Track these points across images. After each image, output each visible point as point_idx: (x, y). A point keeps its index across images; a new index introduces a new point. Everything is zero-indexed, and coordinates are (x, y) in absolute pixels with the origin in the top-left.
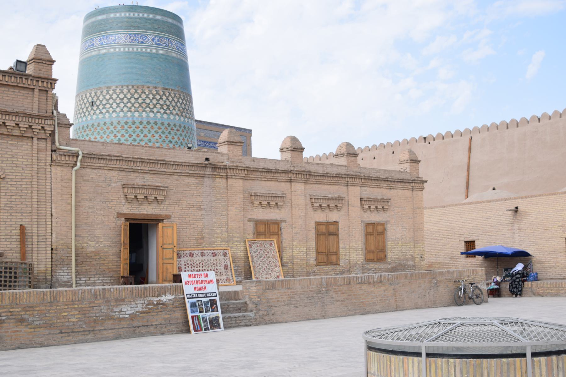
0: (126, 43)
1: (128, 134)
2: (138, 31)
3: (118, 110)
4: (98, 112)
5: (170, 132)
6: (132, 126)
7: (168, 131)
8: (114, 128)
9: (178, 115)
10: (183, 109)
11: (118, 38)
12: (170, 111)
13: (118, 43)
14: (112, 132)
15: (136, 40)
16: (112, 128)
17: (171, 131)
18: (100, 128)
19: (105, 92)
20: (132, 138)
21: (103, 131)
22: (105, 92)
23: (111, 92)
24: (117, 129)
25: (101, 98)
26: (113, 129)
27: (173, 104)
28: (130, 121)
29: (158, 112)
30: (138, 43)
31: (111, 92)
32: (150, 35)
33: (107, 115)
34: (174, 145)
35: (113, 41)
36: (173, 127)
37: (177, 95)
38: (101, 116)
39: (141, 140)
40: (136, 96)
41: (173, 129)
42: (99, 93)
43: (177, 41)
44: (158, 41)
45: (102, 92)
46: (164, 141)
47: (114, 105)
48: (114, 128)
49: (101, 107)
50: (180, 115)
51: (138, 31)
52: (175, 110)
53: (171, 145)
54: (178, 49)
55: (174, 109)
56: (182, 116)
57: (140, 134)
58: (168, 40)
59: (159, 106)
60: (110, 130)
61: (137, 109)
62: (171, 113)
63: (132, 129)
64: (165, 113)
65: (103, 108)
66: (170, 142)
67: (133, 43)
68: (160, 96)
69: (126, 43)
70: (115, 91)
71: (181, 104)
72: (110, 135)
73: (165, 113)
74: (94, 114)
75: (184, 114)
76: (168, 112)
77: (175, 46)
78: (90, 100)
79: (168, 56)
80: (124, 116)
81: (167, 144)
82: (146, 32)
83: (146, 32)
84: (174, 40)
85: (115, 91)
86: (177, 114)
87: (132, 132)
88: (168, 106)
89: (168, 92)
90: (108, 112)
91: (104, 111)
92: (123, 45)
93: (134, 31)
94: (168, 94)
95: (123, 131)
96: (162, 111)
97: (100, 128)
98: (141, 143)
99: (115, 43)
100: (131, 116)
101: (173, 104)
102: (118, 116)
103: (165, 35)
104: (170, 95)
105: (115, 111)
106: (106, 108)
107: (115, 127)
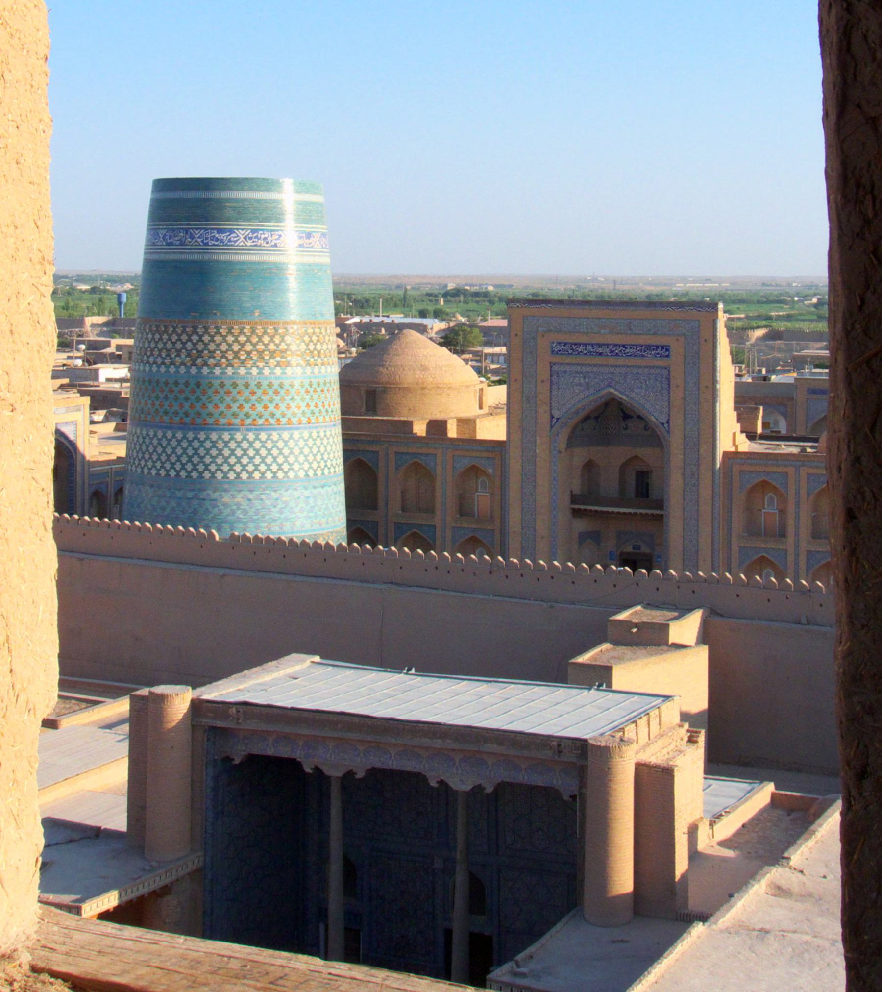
5: (166, 395)
7: (165, 393)
9: (185, 364)
10: (198, 351)
12: (171, 358)
17: (168, 394)
27: (179, 345)
29: (155, 362)
32: (162, 229)
34: (171, 418)
36: (173, 386)
37: (187, 330)
41: (171, 391)
43: (206, 229)
44: (170, 237)
46: (157, 411)
50: (189, 364)
52: (178, 356)
53: (166, 419)
54: (207, 244)
55: (178, 356)
56: (194, 364)
58: (187, 233)
59: (156, 353)
62: (171, 364)
64: (163, 363)
66: (166, 413)
68: (160, 334)
71: (194, 345)
73: (163, 363)
75: (199, 361)
76: (167, 361)
77: (199, 240)
79: (181, 261)
81: (161, 417)
82: (159, 225)
83: (159, 225)
84: (197, 229)
86: (183, 363)
88: (169, 351)
89: (173, 327)
94: (172, 329)
96: (159, 360)
101: (179, 345)
103: (181, 225)
104: (174, 331)
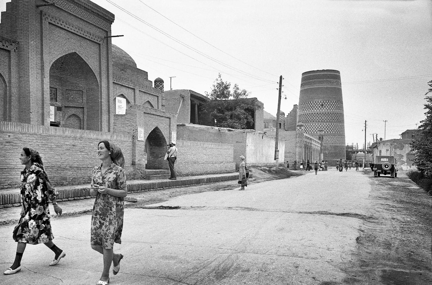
3: (333, 108)
4: (325, 108)
16: (331, 115)
19: (327, 102)
22: (327, 102)
23: (330, 102)
25: (326, 103)
31: (330, 102)
33: (329, 110)
40: (337, 104)
42: (325, 102)
47: (331, 107)
49: (326, 107)
70: (331, 101)
78: (321, 104)
85: (331, 101)
90: (329, 109)
91: (328, 108)
107: (332, 115)
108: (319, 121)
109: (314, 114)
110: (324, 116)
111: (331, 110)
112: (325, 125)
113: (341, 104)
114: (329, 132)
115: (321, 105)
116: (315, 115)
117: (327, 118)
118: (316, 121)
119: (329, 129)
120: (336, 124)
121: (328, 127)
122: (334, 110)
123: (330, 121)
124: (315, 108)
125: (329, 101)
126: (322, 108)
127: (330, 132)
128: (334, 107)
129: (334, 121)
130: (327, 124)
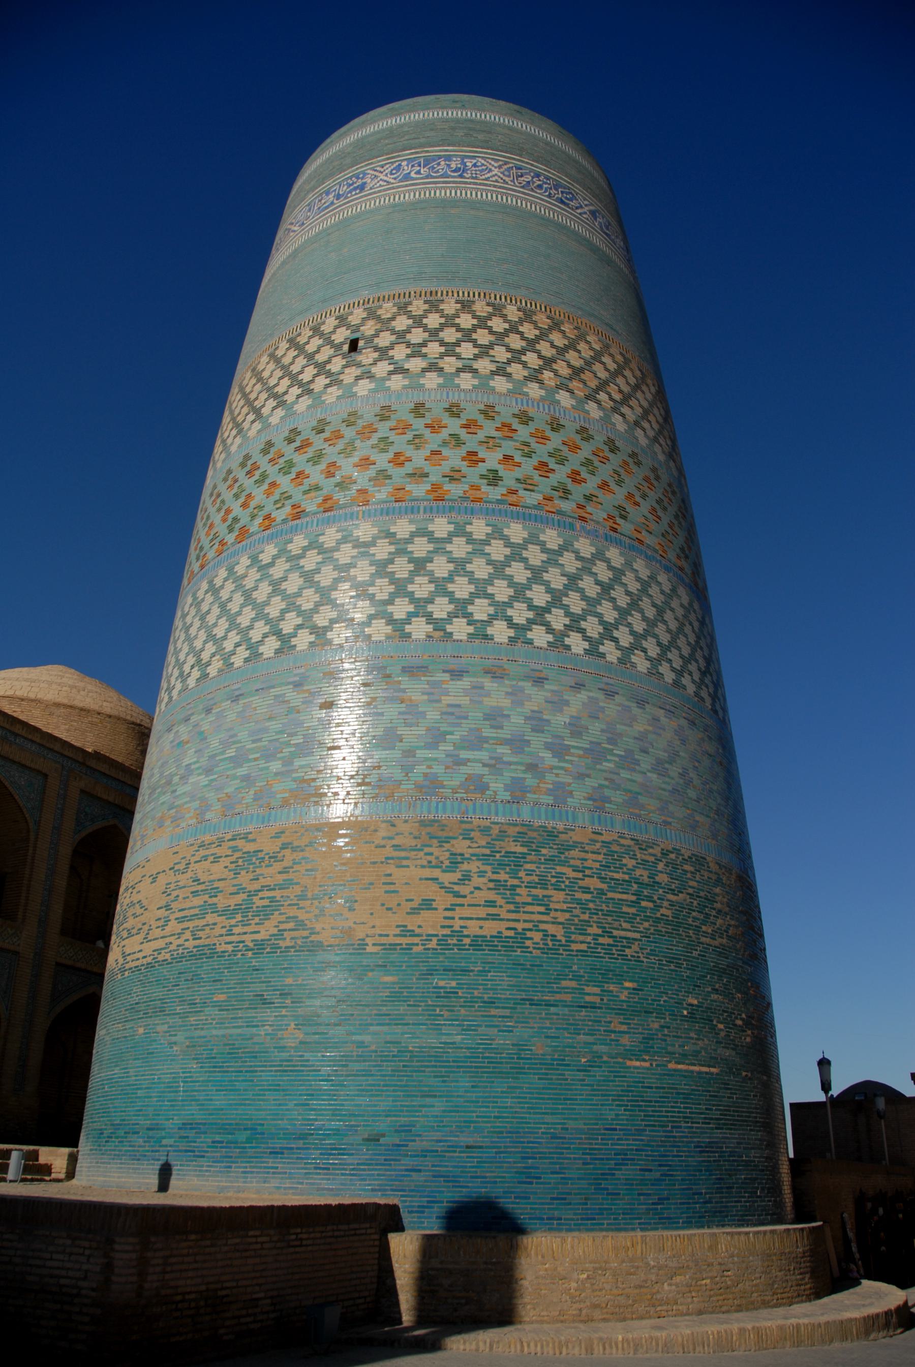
0: (507, 183)
1: (534, 461)
2: (545, 170)
4: (382, 368)
6: (549, 433)
8: (464, 426)
11: (475, 165)
13: (476, 178)
14: (457, 441)
15: (540, 187)
16: (454, 425)
18: (392, 423)
19: (419, 306)
20: (554, 479)
21: (409, 436)
23: (450, 307)
24: (481, 435)
26: (463, 433)
28: (541, 416)
30: (550, 196)
31: (450, 307)
35: (455, 171)
38: (397, 382)
39: (589, 498)
45: (403, 309)
48: (464, 426)
51: (545, 170)
57: (584, 474)
60: (444, 434)
61: (558, 379)
63: (550, 446)
65: (409, 356)
67: (532, 190)
69: (505, 182)
72: (446, 452)
74: (358, 378)
78: (342, 335)
80: (509, 391)
85: (466, 306)
87: (550, 455)
90: (433, 367)
91: (416, 364)
92: (495, 186)
93: (532, 165)
95: (511, 443)
97: (392, 423)
98: (589, 509)
99: (461, 176)
100: (542, 399)
102: (483, 386)
105: (468, 369)
106: (425, 356)
108: (298, 513)
109: (257, 457)
110: (363, 448)
111: (466, 381)
112: (363, 547)
113: (606, 359)
114: (419, 629)
115: (338, 347)
116: (264, 463)
117: (398, 460)
118: (268, 517)
119: (421, 588)
120: (533, 539)
121: (402, 568)
122: (500, 384)
123: (437, 495)
124: (276, 396)
125: (434, 306)
126: (349, 376)
127: (439, 625)
128: (501, 354)
129: (495, 493)
130: (403, 528)
